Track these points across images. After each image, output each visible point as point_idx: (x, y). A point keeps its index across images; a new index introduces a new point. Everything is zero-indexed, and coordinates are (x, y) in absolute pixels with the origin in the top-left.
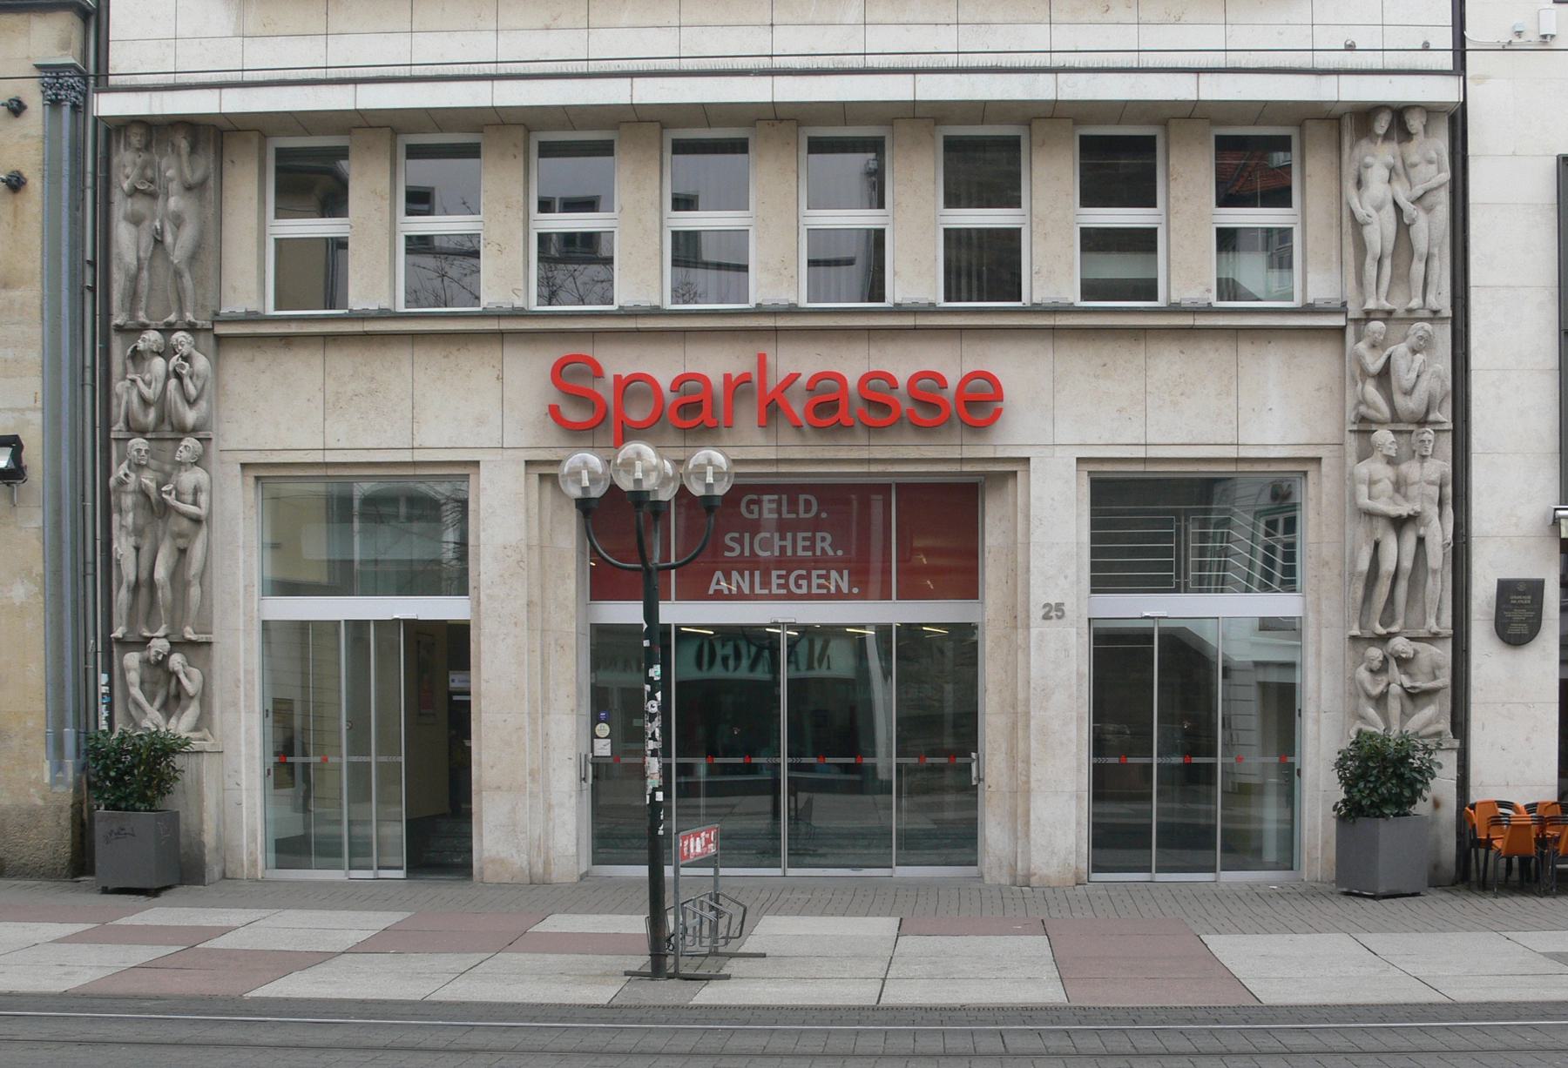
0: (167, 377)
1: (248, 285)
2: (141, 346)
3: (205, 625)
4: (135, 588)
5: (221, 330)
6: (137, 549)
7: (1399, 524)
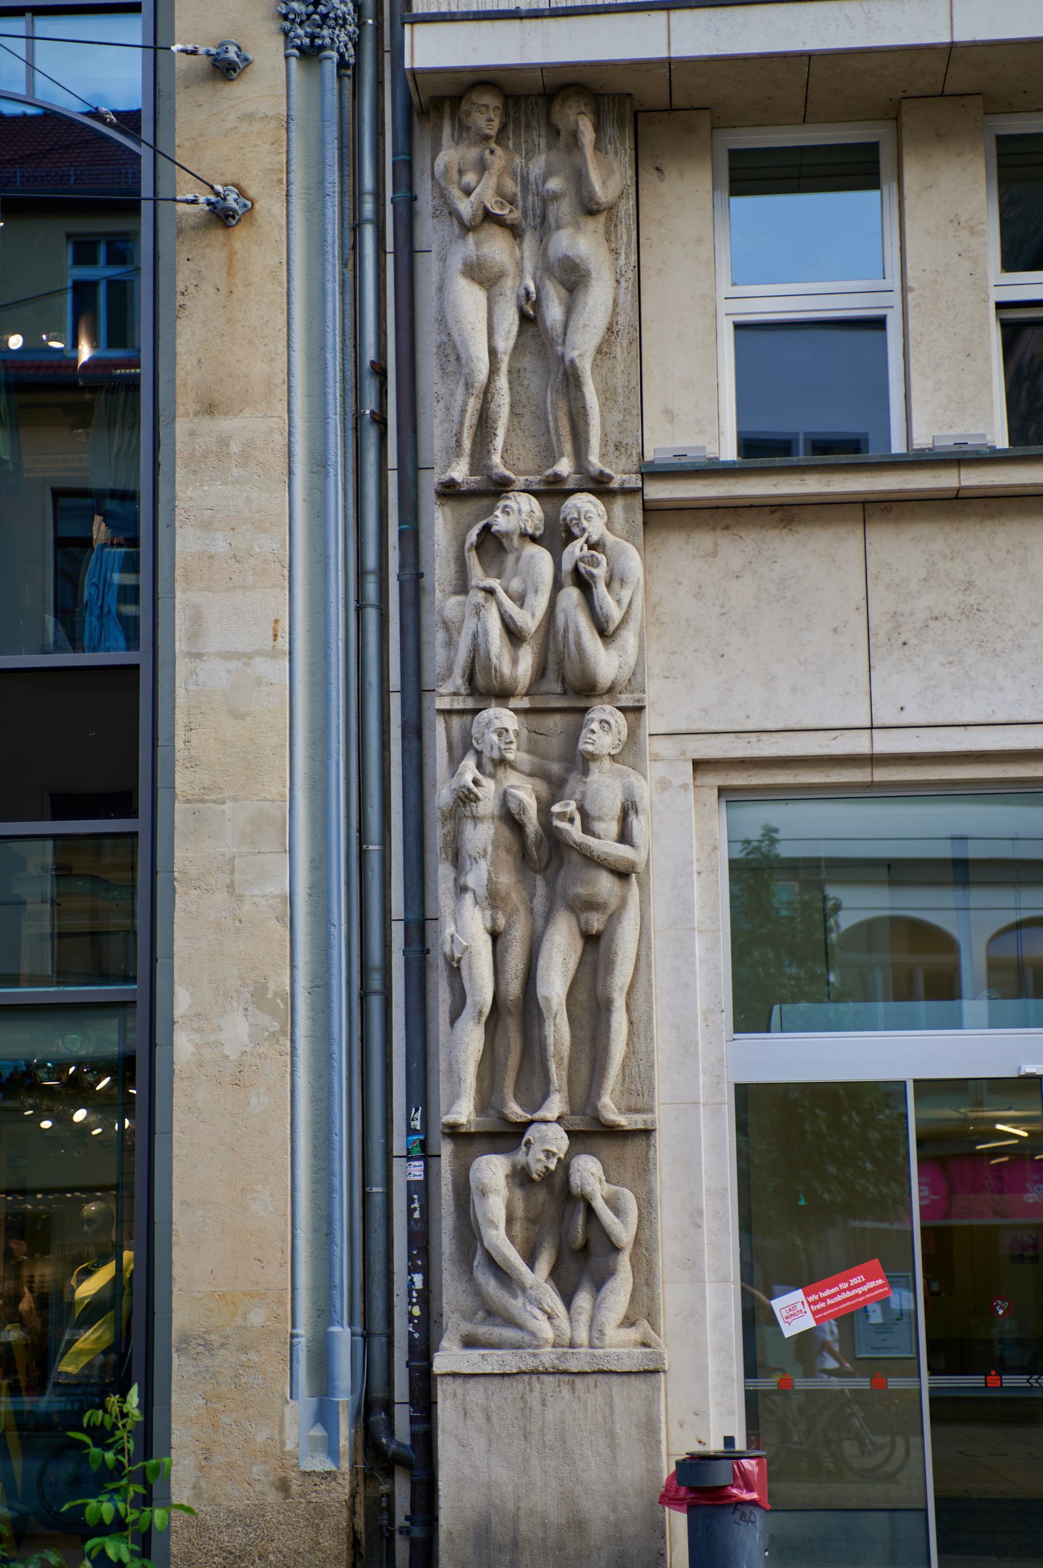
0: (557, 586)
1: (698, 411)
2: (501, 522)
3: (639, 1092)
5: (658, 491)
6: (495, 936)
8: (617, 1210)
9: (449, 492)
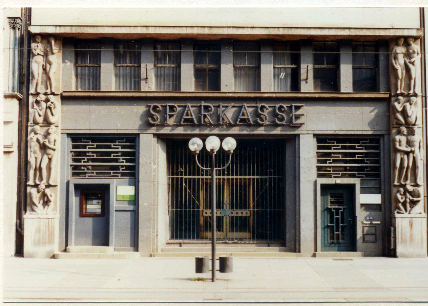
0: (47, 108)
2: (39, 99)
4: (35, 170)
7: (407, 153)
8: (51, 196)
9: (32, 94)
